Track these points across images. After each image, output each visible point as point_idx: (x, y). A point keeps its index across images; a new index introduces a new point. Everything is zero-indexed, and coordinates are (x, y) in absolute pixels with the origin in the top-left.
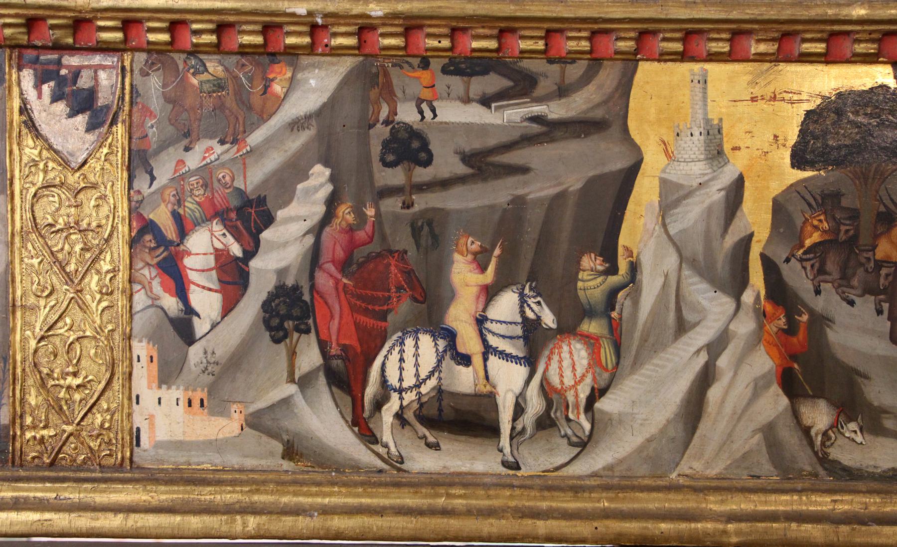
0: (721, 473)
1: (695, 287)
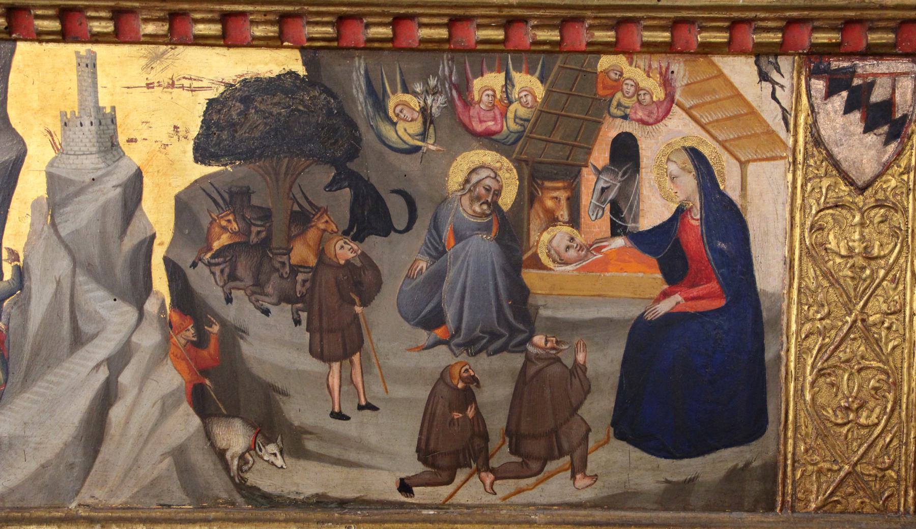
0: (126, 503)
1: (92, 294)
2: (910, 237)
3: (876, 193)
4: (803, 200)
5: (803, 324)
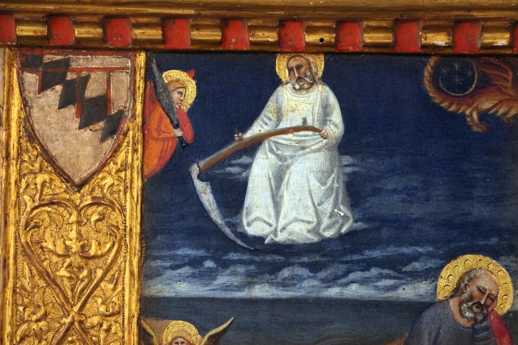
2: (128, 236)
3: (93, 190)
4: (18, 197)
5: (18, 326)
